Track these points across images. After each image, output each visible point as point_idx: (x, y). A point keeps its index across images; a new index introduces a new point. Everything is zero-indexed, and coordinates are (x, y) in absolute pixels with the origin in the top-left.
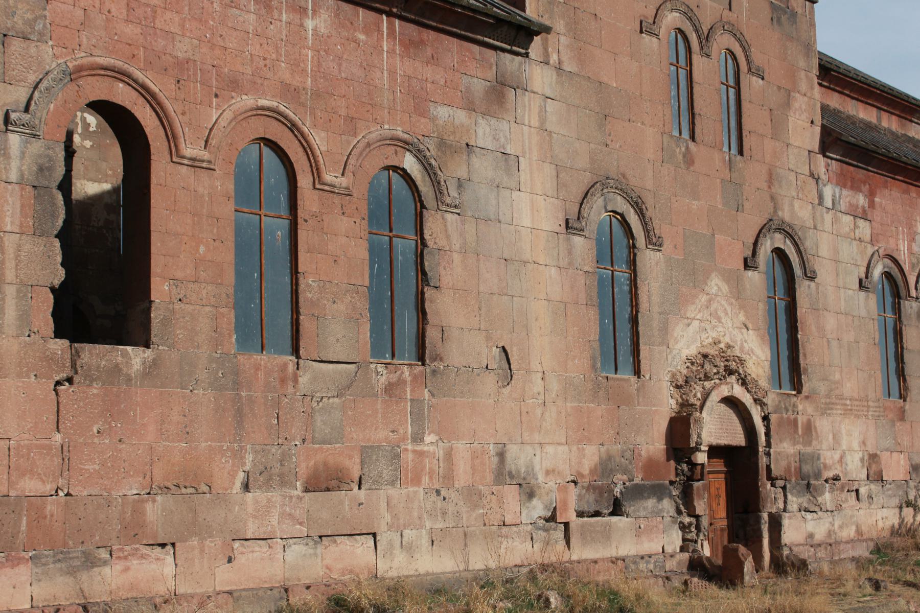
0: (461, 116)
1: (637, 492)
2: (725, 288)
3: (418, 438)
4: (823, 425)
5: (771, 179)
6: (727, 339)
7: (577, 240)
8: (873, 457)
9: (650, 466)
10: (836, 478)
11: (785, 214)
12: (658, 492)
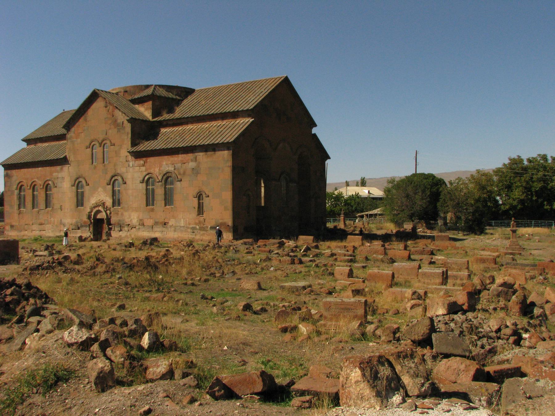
0: (56, 174)
1: (82, 226)
2: (102, 190)
3: (50, 219)
4: (126, 214)
5: (115, 165)
6: (102, 199)
7: (73, 187)
8: (141, 220)
9: (85, 222)
10: (129, 225)
11: (119, 171)
12: (86, 226)
